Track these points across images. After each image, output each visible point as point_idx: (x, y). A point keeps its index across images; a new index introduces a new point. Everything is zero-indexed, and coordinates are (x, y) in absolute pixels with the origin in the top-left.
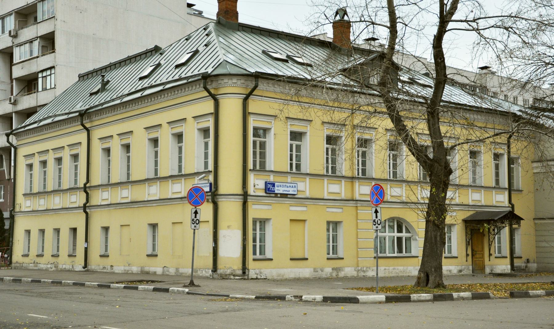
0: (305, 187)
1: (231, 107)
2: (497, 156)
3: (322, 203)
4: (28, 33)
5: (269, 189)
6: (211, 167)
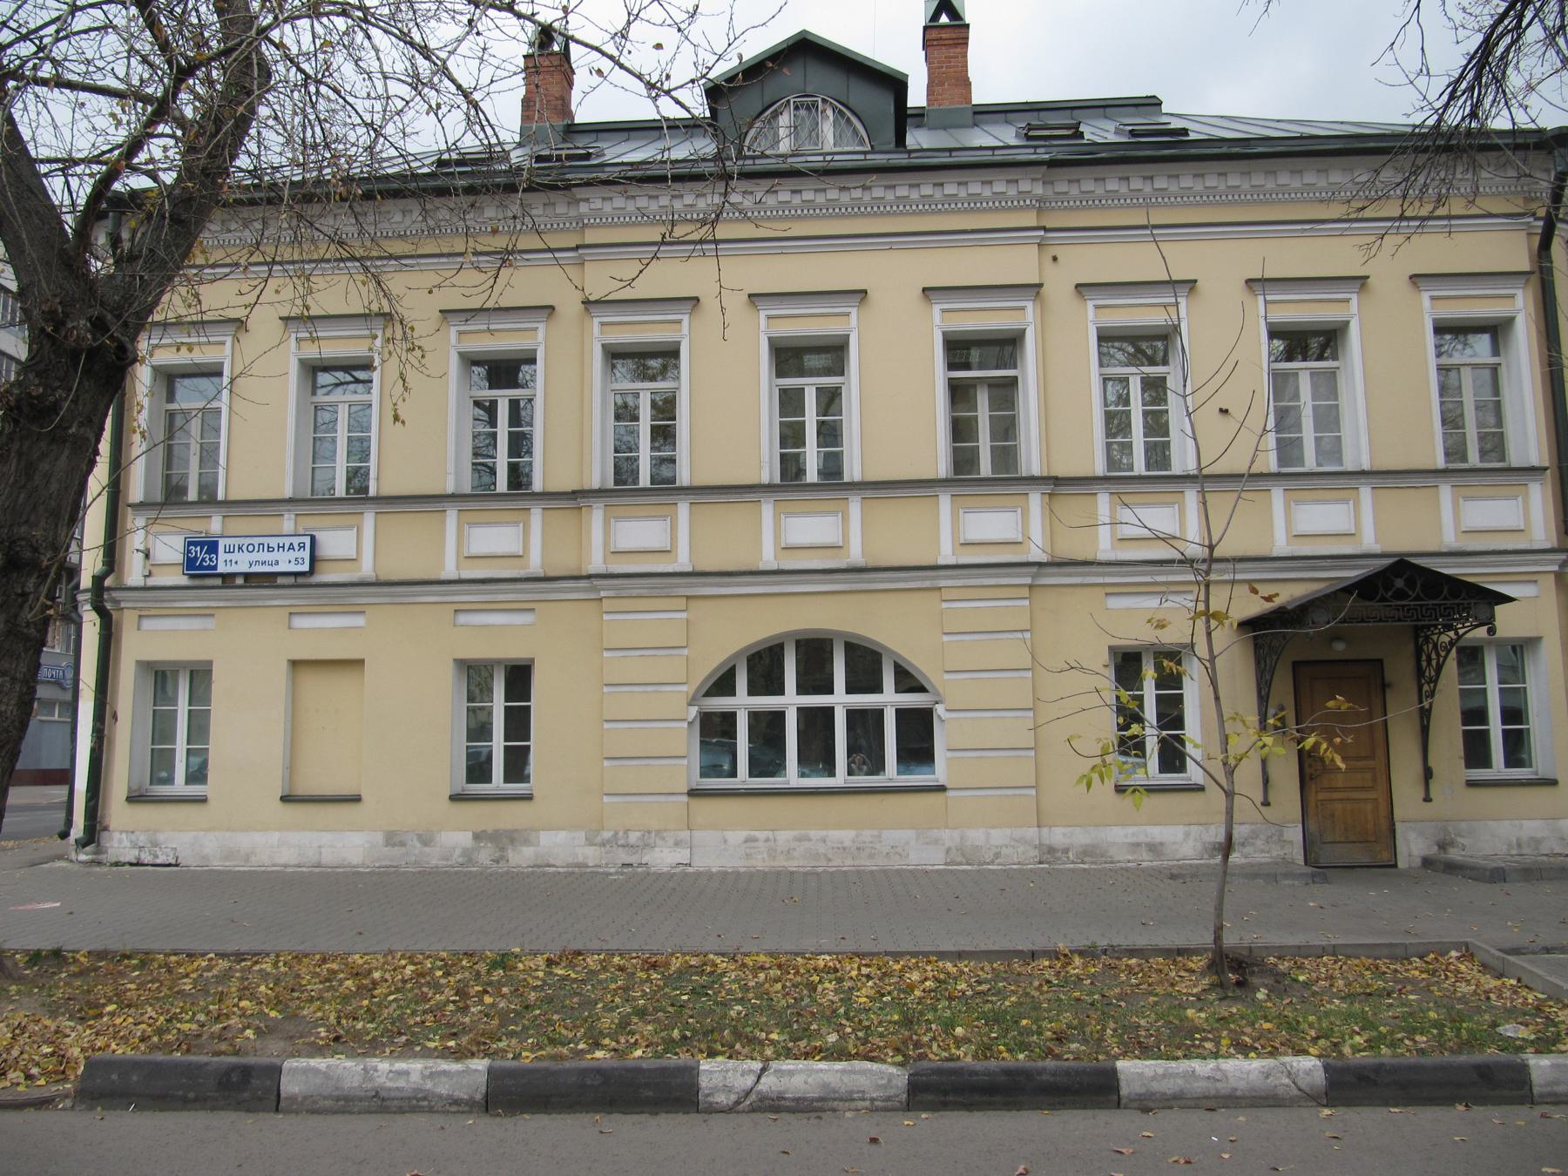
3: (430, 596)
5: (199, 562)
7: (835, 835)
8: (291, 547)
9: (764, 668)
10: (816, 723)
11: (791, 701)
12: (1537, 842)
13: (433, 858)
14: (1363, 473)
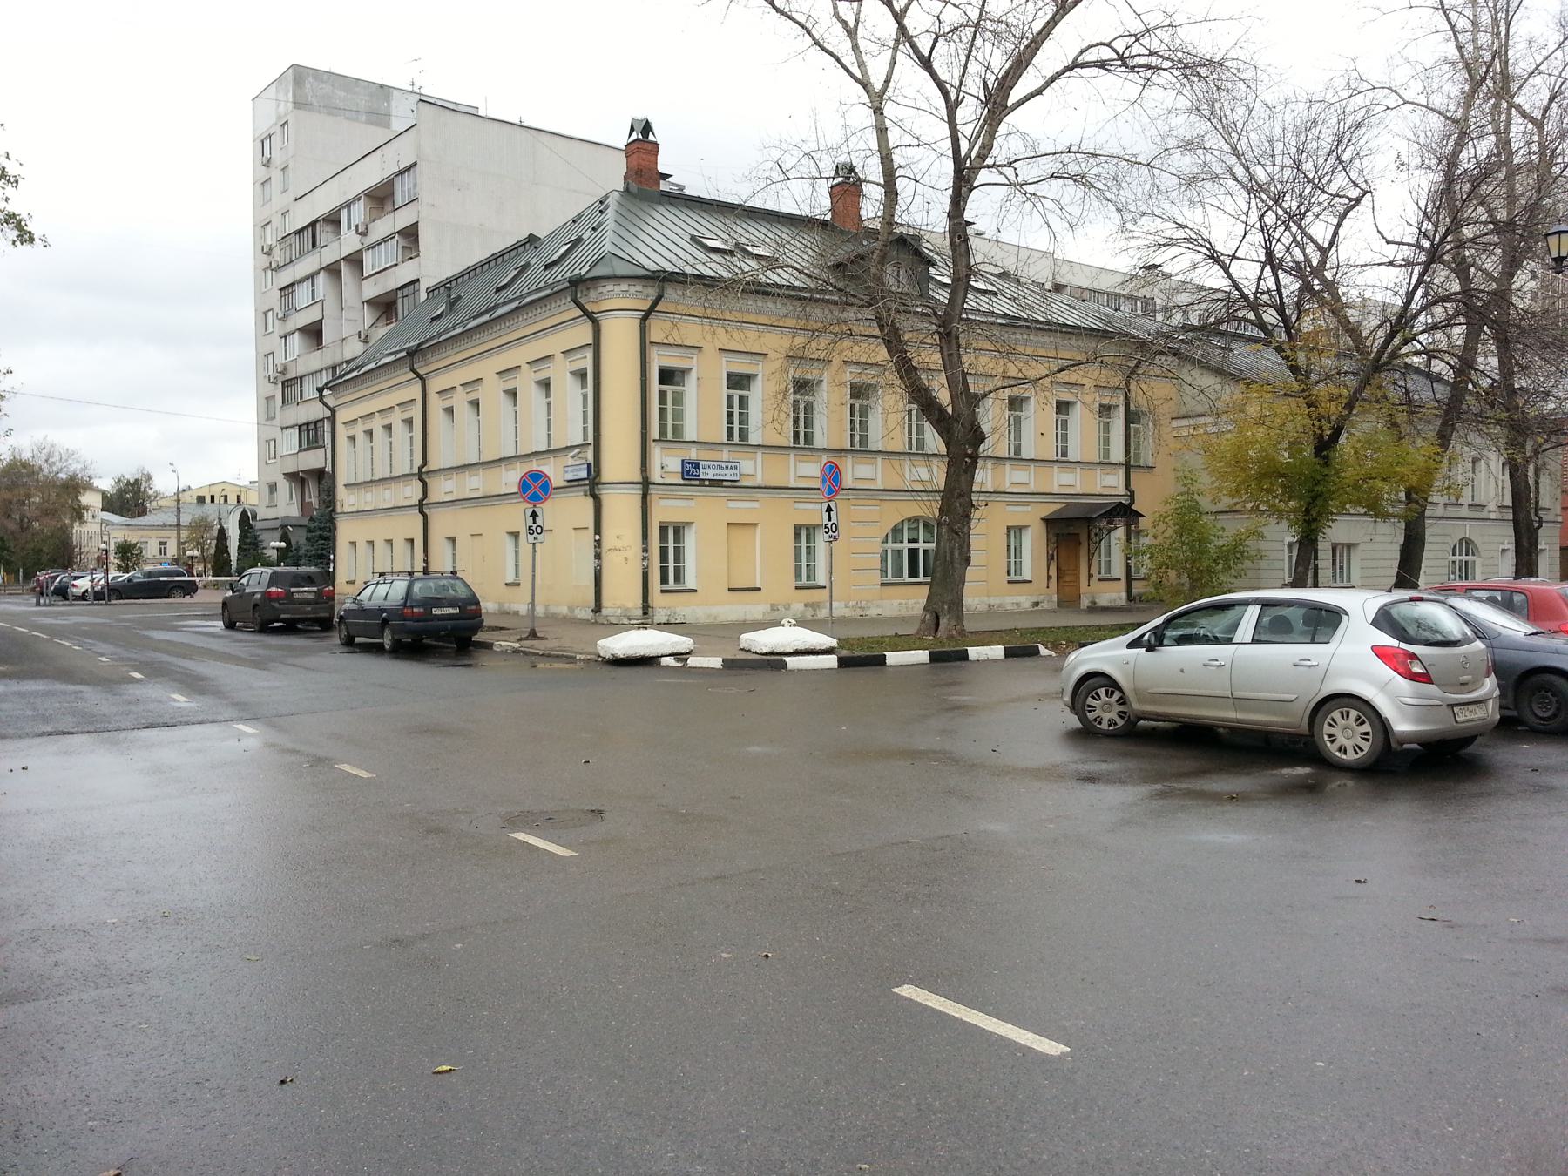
0: (754, 468)
1: (620, 335)
2: (1106, 410)
4: (384, 226)
5: (690, 472)
6: (591, 440)
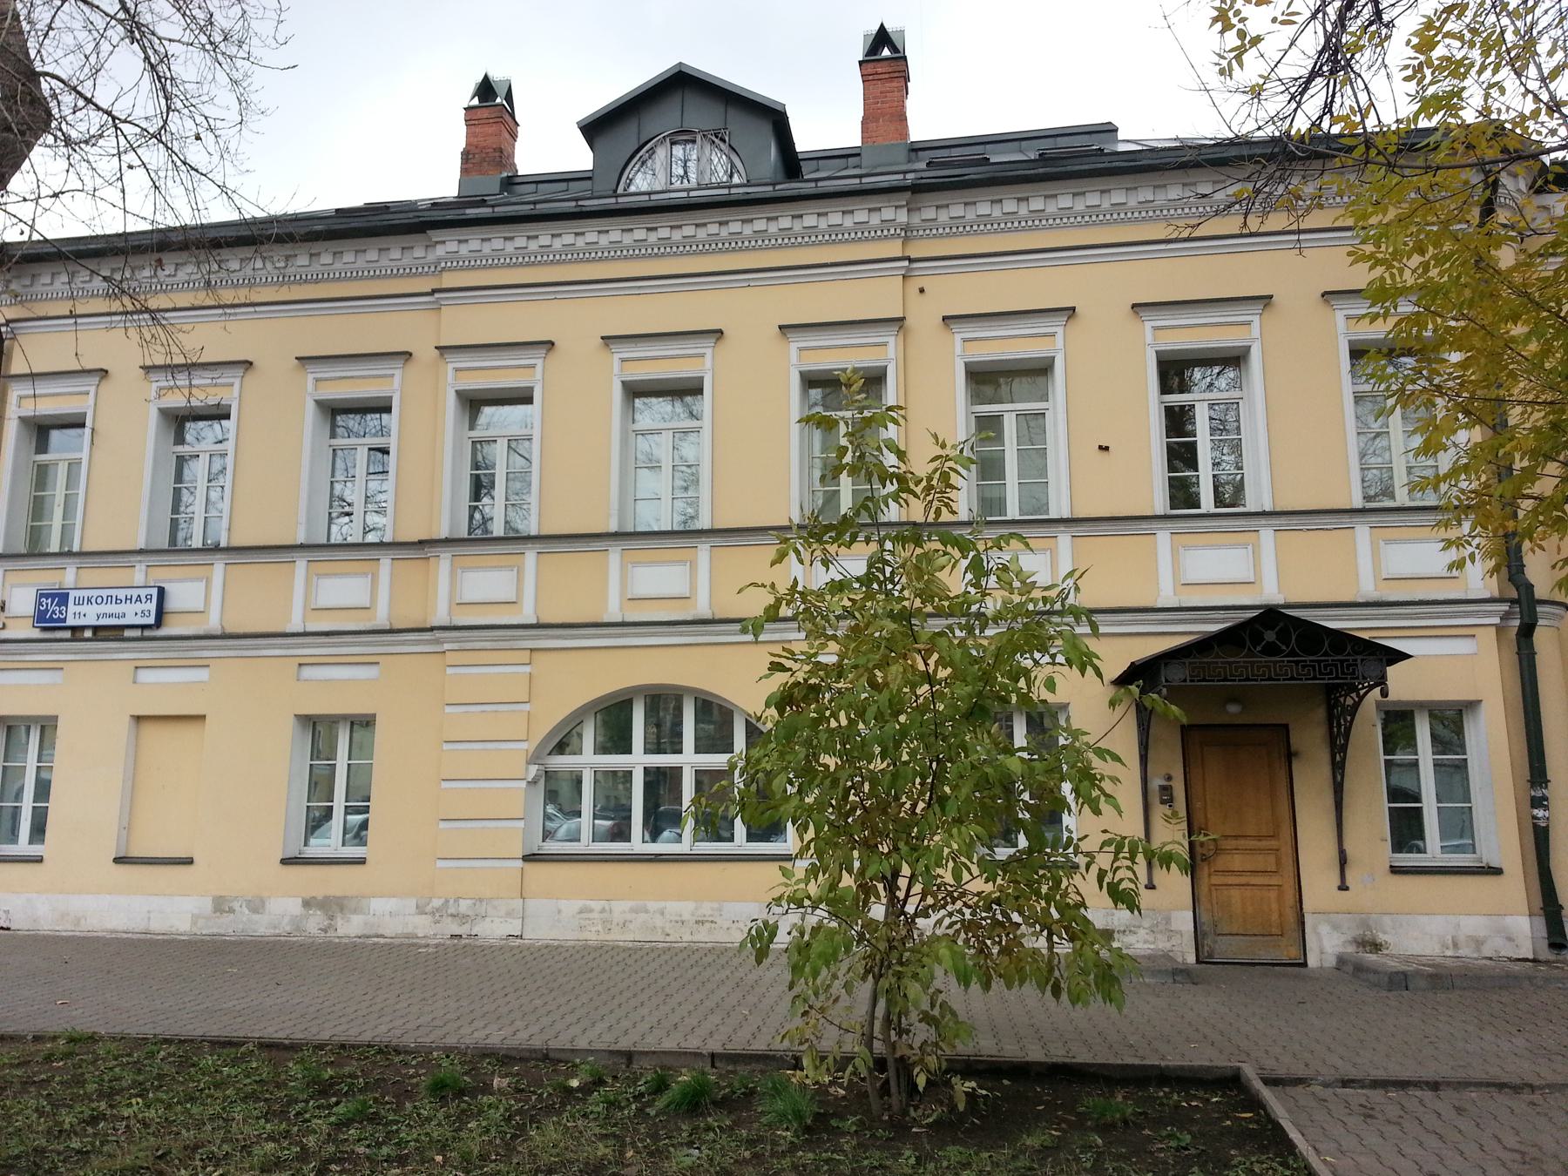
3: (274, 650)
7: (673, 907)
8: (139, 599)
9: (613, 721)
10: (661, 783)
11: (638, 760)
12: (1478, 943)
13: (261, 926)
14: (1264, 514)
